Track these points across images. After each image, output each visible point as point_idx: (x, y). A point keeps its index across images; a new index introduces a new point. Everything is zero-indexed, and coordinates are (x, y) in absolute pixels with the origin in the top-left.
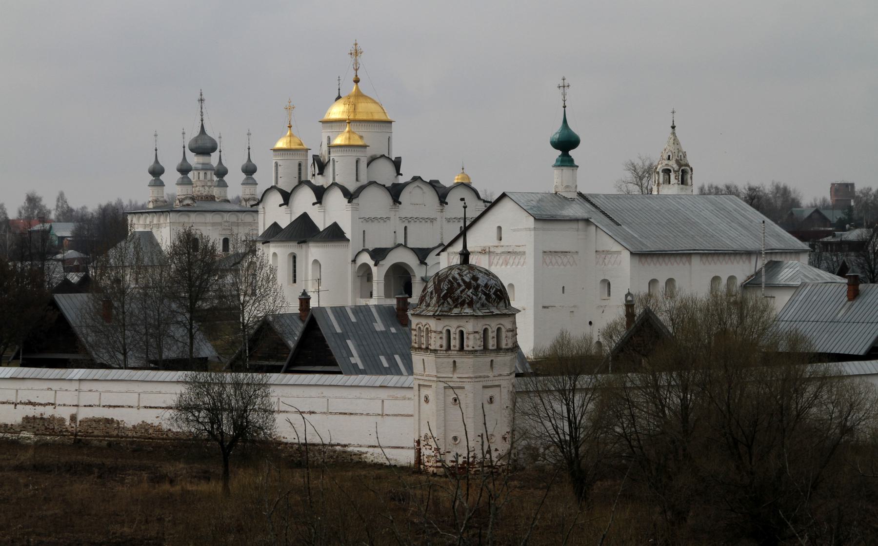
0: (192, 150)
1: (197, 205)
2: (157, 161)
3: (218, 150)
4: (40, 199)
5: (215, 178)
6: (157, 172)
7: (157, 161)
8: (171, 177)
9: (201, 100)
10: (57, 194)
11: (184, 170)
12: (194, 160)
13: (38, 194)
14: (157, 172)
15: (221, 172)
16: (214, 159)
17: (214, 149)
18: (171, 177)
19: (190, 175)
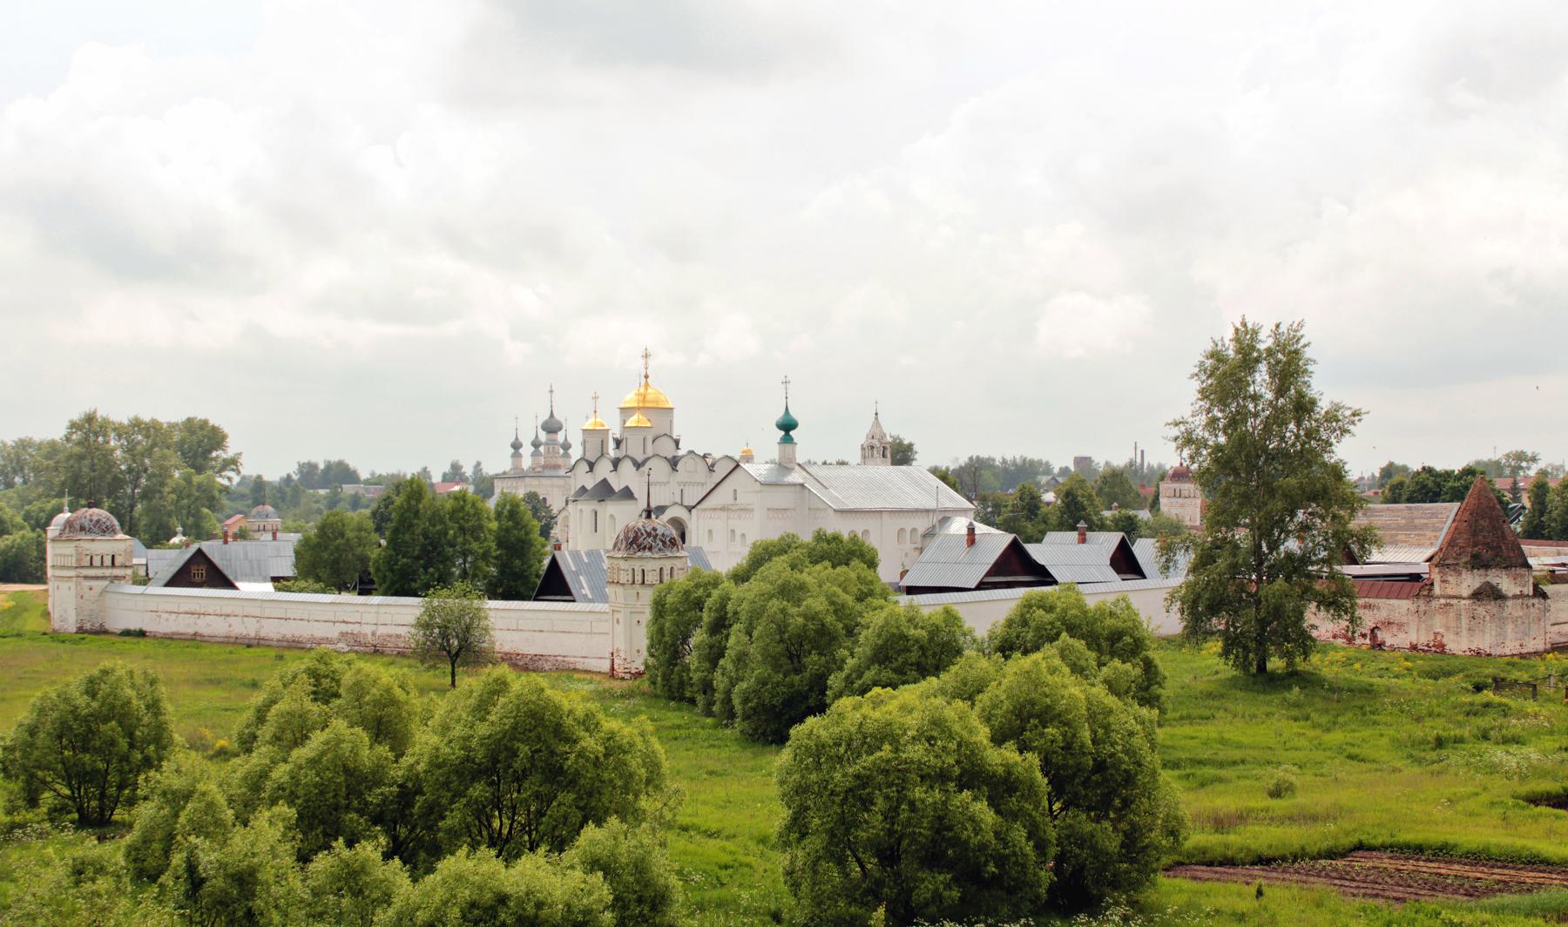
0: (544, 429)
1: (547, 473)
2: (517, 439)
3: (563, 430)
4: (462, 467)
5: (561, 451)
6: (516, 446)
7: (517, 439)
8: (527, 450)
9: (551, 391)
10: (475, 463)
11: (536, 444)
12: (543, 436)
13: (461, 463)
14: (516, 446)
15: (566, 446)
16: (560, 437)
17: (560, 429)
18: (527, 450)
19: (542, 449)
